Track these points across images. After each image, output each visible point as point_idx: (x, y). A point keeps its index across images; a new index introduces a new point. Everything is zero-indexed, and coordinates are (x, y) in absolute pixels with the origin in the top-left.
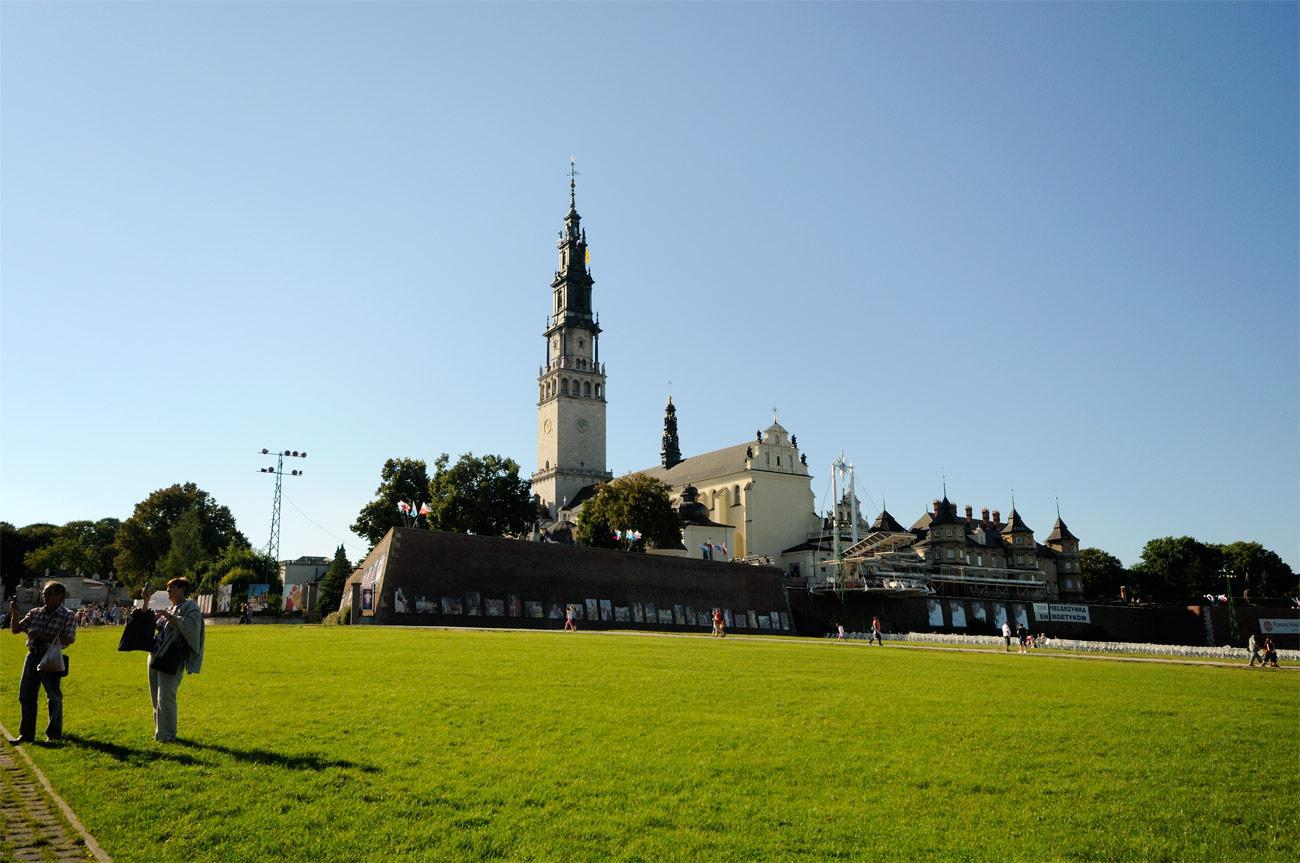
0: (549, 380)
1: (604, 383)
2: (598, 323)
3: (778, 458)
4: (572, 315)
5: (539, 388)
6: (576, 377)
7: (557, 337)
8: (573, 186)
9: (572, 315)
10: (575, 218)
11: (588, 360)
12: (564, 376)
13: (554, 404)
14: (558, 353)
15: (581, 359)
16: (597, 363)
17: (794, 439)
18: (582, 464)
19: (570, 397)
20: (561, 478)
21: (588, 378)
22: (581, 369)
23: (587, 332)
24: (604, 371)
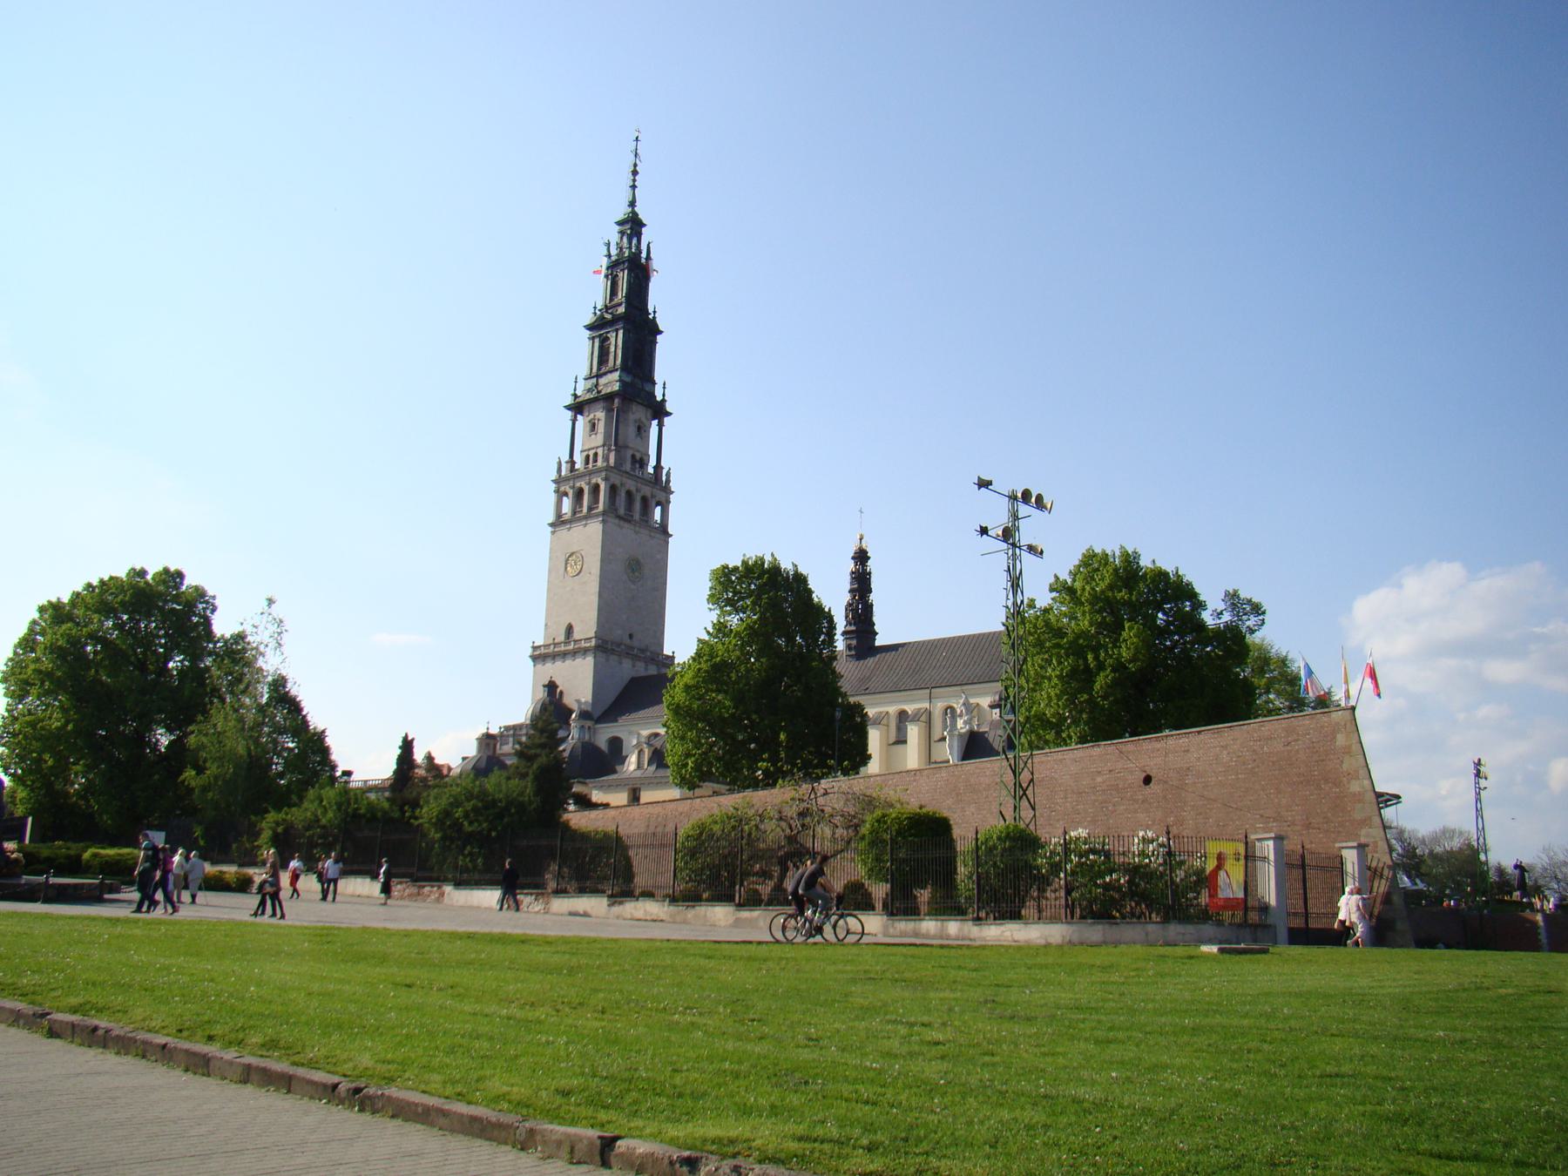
0: (582, 484)
1: (669, 502)
2: (664, 401)
4: (628, 379)
5: (553, 498)
6: (631, 485)
8: (635, 173)
10: (633, 225)
13: (595, 529)
14: (599, 439)
15: (638, 456)
16: (658, 467)
18: (631, 636)
21: (647, 490)
23: (649, 413)
24: (668, 481)
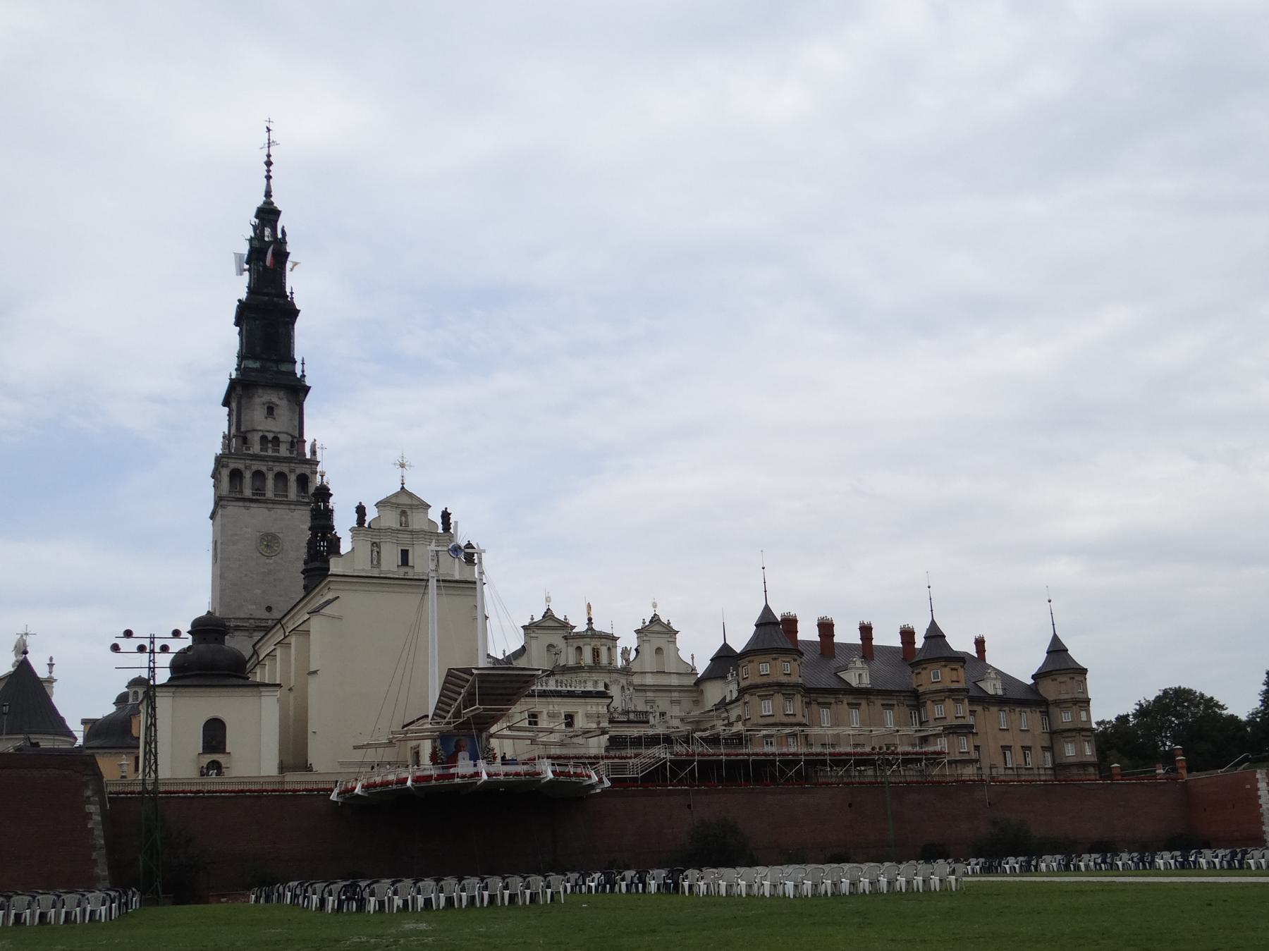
2: (303, 376)
3: (405, 554)
4: (257, 365)
6: (257, 466)
7: (234, 405)
8: (269, 164)
9: (257, 365)
10: (268, 214)
11: (283, 437)
15: (270, 436)
17: (446, 516)
18: (269, 609)
22: (270, 453)
23: (281, 394)
24: (314, 452)
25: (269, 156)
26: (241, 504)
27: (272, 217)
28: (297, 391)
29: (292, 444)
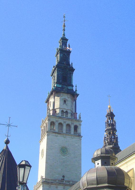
2: (76, 91)
4: (60, 86)
6: (60, 121)
7: (51, 100)
8: (64, 26)
9: (60, 86)
10: (64, 41)
11: (69, 111)
12: (52, 120)
15: (65, 111)
16: (76, 113)
19: (55, 133)
20: (47, 186)
21: (69, 122)
23: (69, 96)
24: (80, 118)
25: (64, 24)
26: (54, 134)
27: (65, 41)
28: (74, 95)
29: (72, 115)
